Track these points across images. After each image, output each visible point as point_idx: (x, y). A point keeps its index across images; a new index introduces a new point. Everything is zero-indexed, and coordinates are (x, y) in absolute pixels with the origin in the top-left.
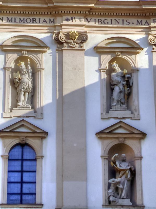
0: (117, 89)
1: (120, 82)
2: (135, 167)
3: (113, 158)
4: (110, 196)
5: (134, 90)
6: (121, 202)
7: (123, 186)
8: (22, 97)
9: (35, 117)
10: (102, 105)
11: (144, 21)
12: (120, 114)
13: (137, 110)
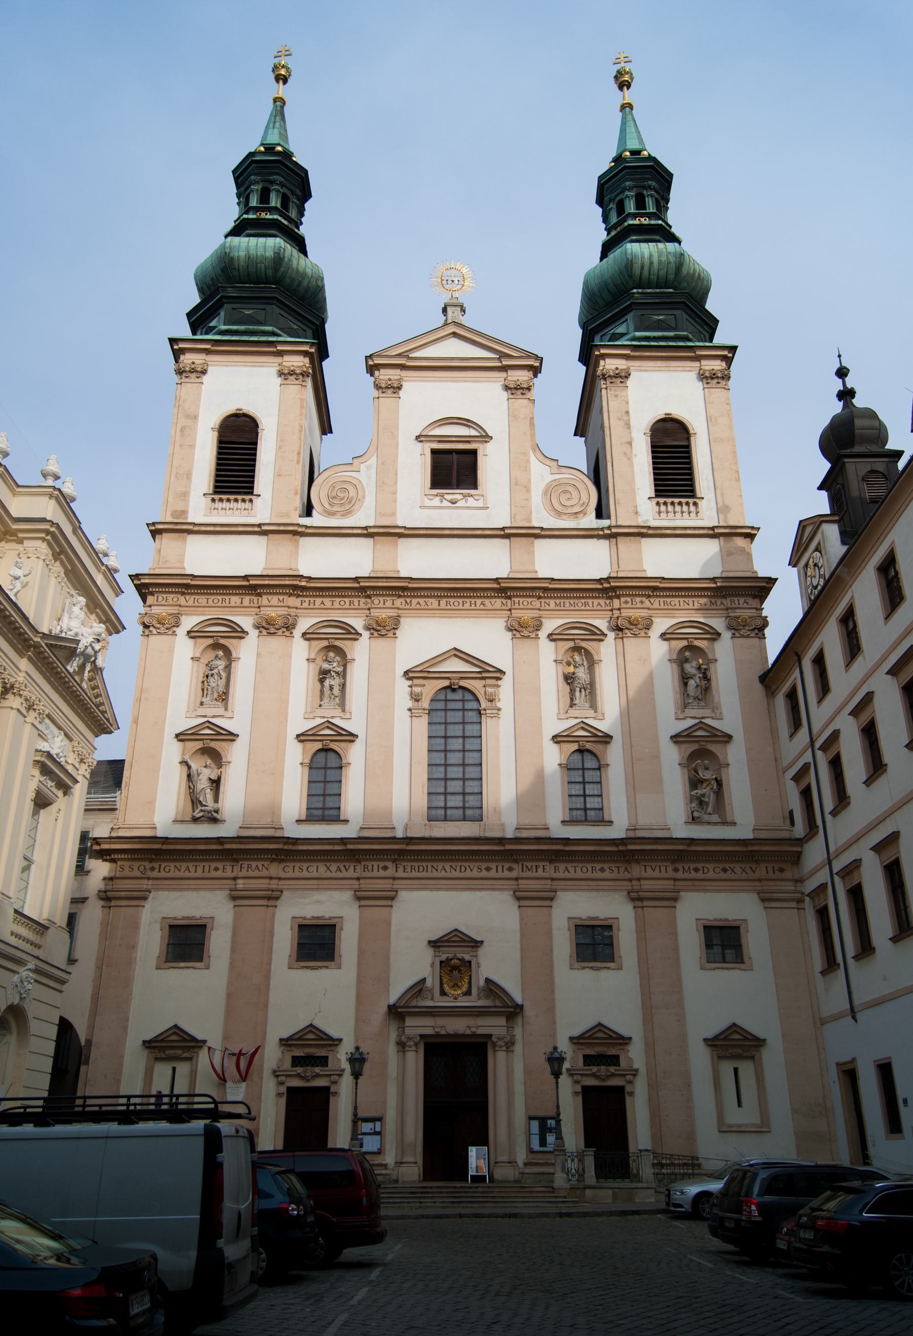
0: (692, 683)
1: (695, 675)
2: (721, 777)
5: (713, 683)
6: (706, 817)
7: (709, 799)
8: (577, 693)
9: (595, 718)
10: (676, 703)
11: (719, 602)
12: (699, 713)
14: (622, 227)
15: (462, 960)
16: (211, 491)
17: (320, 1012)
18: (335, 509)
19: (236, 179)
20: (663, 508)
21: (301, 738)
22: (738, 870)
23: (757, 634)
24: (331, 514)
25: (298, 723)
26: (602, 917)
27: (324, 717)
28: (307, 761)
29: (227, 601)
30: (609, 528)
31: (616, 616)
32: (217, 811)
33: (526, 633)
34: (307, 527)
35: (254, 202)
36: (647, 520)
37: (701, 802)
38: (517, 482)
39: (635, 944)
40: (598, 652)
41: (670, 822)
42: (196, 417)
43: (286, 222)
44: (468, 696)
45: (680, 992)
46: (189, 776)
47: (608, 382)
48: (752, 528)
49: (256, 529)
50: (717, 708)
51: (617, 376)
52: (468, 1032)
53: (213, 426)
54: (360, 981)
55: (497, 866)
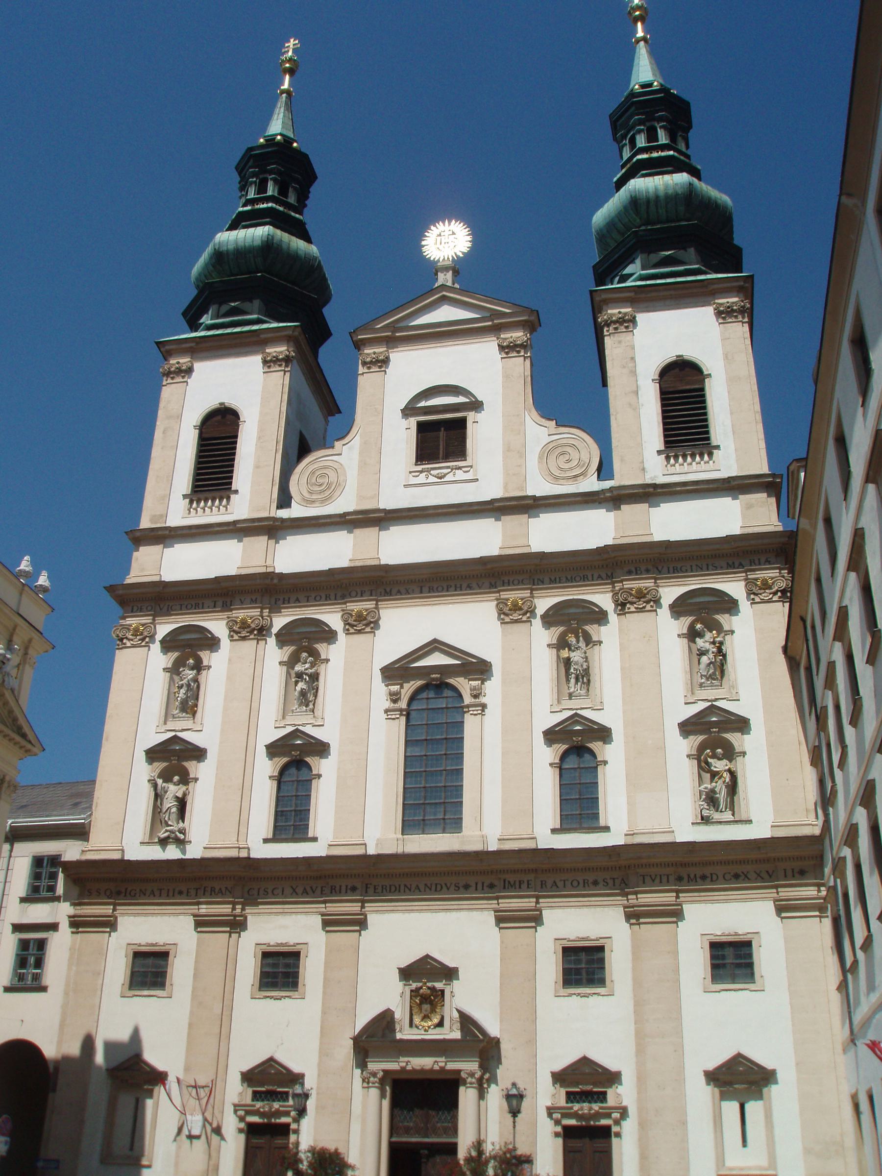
1: (707, 651)
4: (703, 809)
14: (631, 163)
15: (433, 989)
17: (282, 1044)
18: (314, 497)
19: (240, 174)
20: (672, 461)
22: (752, 875)
23: (780, 597)
24: (309, 502)
25: (270, 733)
26: (593, 938)
27: (296, 725)
28: (276, 774)
29: (201, 606)
30: (611, 489)
31: (617, 588)
32: (183, 831)
33: (516, 616)
34: (282, 520)
36: (655, 477)
37: (711, 799)
38: (509, 447)
39: (630, 965)
40: (599, 632)
42: (180, 417)
43: (281, 209)
45: (679, 1018)
47: (611, 328)
49: (231, 527)
50: (733, 687)
52: (436, 1067)
53: (195, 424)
54: (324, 1013)
55: (477, 884)
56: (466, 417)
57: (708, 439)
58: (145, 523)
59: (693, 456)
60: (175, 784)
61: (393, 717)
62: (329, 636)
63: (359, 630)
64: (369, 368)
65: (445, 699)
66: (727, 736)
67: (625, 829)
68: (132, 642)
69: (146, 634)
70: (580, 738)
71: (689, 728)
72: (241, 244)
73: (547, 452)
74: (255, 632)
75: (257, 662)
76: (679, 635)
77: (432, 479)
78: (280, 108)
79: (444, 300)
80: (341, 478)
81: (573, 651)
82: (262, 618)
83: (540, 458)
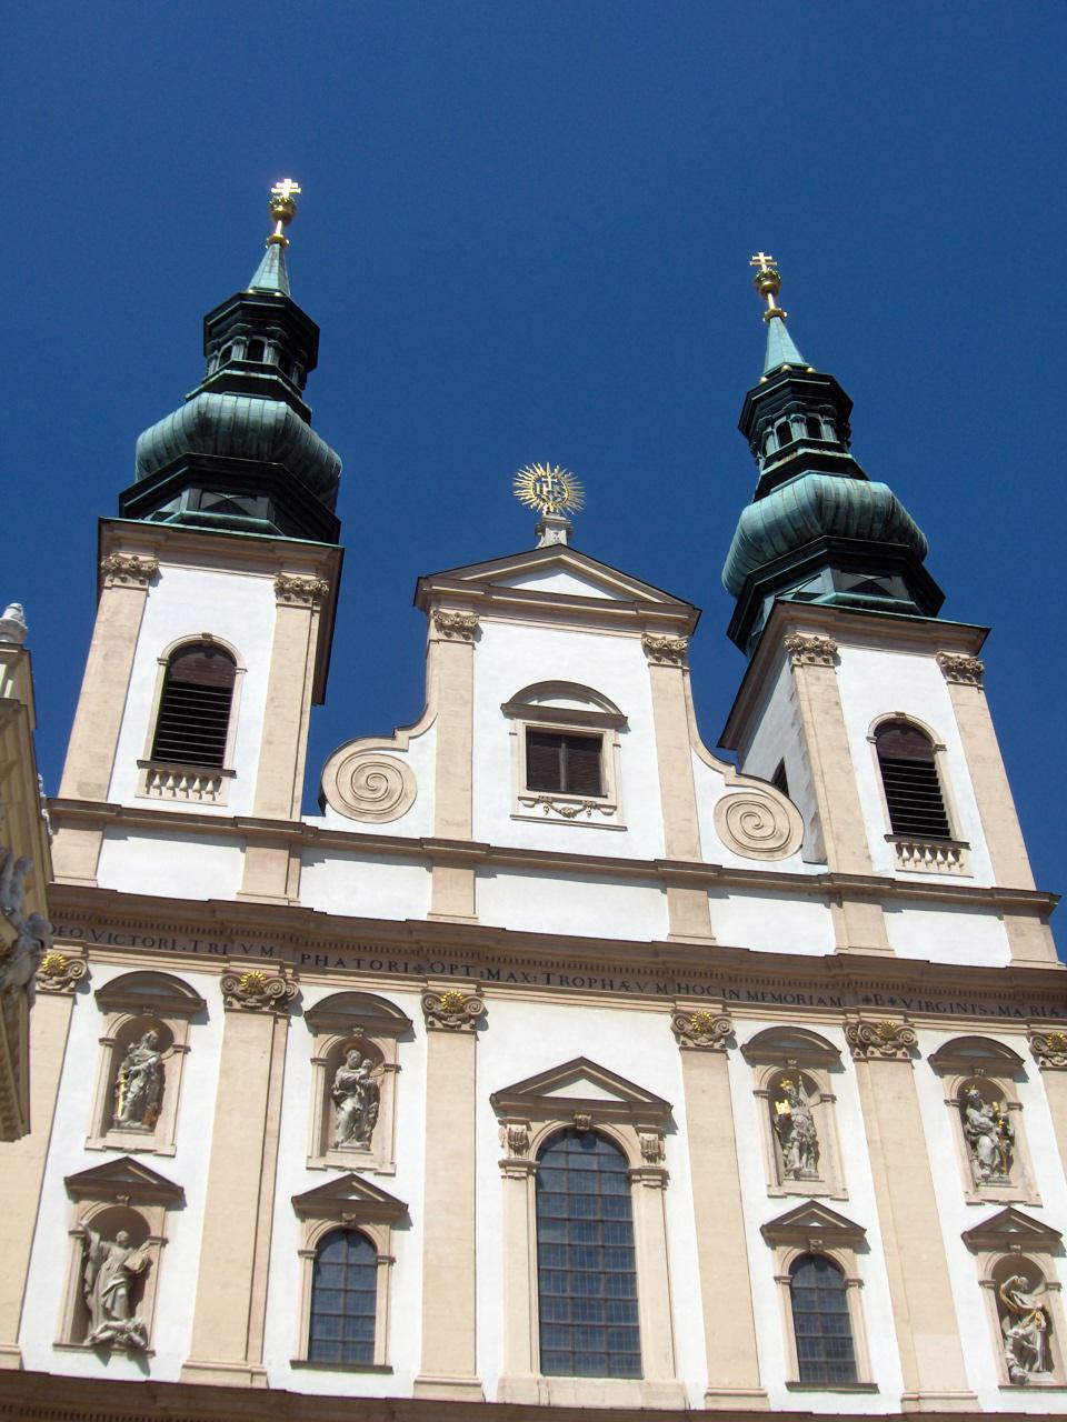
0: (986, 1143)
1: (990, 1129)
3: (1004, 1286)
4: (1012, 1366)
6: (1033, 1378)
12: (1003, 1193)
13: (1029, 1186)
14: (794, 455)
16: (148, 759)
18: (365, 806)
20: (905, 854)
21: (306, 1205)
24: (354, 813)
25: (298, 1174)
27: (346, 1169)
28: (312, 1248)
29: (169, 944)
30: (829, 877)
32: (142, 1332)
33: (703, 1040)
35: (238, 355)
36: (886, 870)
37: (1023, 1353)
41: (975, 1388)
44: (601, 1147)
46: (85, 1260)
48: (1051, 896)
51: (819, 650)
53: (160, 656)
56: (602, 735)
57: (947, 832)
58: (67, 791)
59: (933, 852)
60: (120, 1244)
61: (517, 1175)
62: (401, 1028)
63: (452, 1027)
64: (448, 635)
65: (596, 1158)
66: (1032, 1256)
67: (900, 1391)
68: (43, 985)
69: (70, 974)
70: (820, 1242)
71: (980, 1241)
72: (242, 415)
73: (728, 807)
74: (273, 1003)
75: (276, 1050)
76: (946, 1102)
77: (553, 815)
78: (272, 260)
79: (559, 567)
80: (409, 787)
81: (793, 1106)
82: (285, 980)
83: (717, 815)
